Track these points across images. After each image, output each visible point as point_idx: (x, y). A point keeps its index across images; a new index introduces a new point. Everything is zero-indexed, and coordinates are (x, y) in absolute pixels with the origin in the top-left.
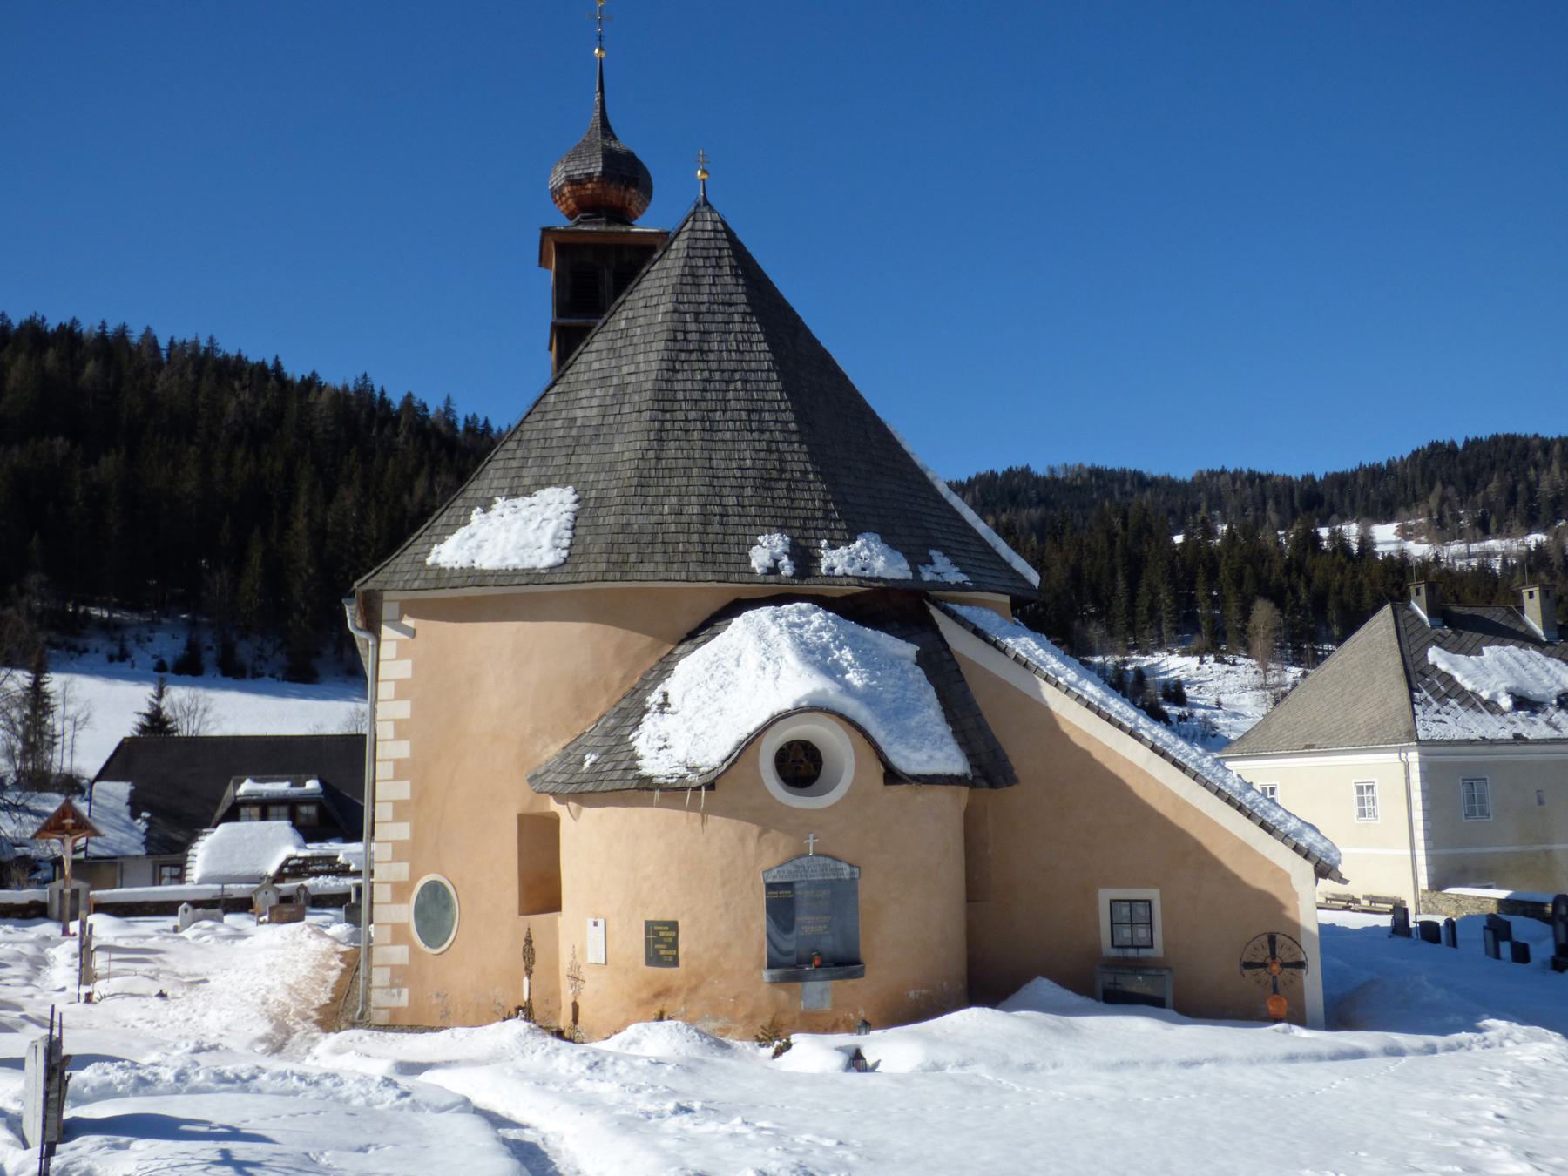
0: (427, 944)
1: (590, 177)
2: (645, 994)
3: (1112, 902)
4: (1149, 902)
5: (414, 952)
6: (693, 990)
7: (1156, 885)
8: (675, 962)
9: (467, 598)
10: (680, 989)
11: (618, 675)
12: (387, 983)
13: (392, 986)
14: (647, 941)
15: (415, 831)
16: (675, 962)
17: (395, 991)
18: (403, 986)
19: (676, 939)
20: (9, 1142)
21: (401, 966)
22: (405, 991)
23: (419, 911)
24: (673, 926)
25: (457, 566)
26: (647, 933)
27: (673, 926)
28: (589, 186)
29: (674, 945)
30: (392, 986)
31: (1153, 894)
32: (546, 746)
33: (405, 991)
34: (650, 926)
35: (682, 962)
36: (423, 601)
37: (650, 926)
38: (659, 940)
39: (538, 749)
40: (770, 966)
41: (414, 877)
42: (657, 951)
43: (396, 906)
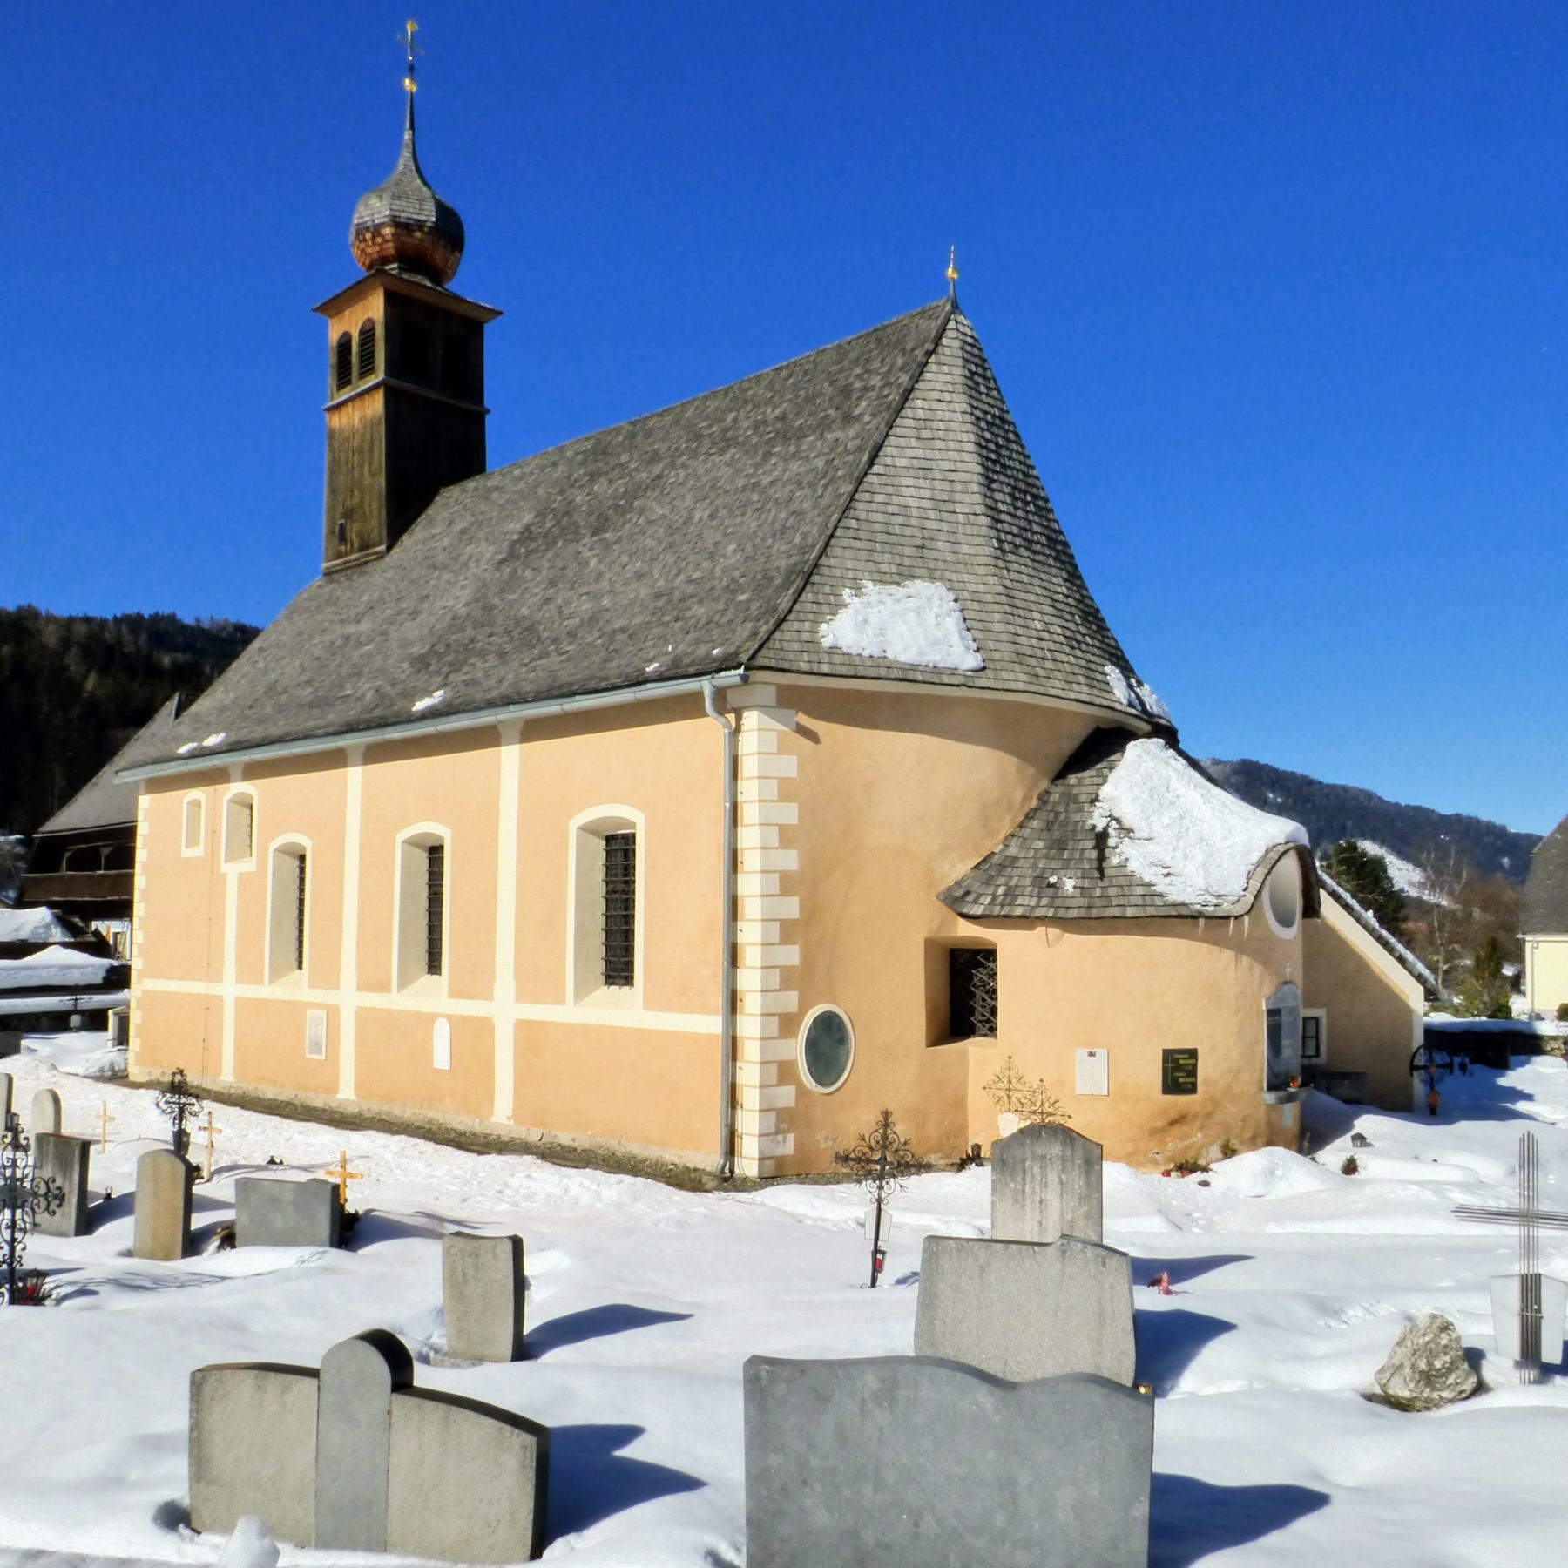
0: (820, 1082)
1: (420, 225)
2: (1159, 1123)
3: (1305, 1019)
4: (1317, 1020)
5: (802, 1092)
6: (1209, 1115)
7: (1324, 1005)
8: (1192, 1089)
9: (859, 692)
10: (1196, 1116)
11: (1019, 794)
12: (773, 1130)
13: (778, 1132)
14: (1165, 1070)
15: (806, 955)
16: (1192, 1089)
17: (780, 1138)
18: (789, 1131)
19: (1195, 1066)
20: (629, 1433)
21: (788, 1109)
22: (791, 1137)
23: (812, 1046)
24: (1193, 1053)
25: (866, 653)
26: (1165, 1060)
27: (1193, 1053)
28: (418, 234)
29: (1193, 1072)
30: (778, 1132)
31: (1320, 1013)
32: (953, 865)
33: (791, 1137)
34: (1168, 1055)
35: (1200, 1088)
36: (806, 689)
37: (1168, 1055)
38: (1179, 1068)
39: (946, 868)
40: (1271, 1088)
41: (803, 1008)
42: (1175, 1080)
43: (783, 1041)
